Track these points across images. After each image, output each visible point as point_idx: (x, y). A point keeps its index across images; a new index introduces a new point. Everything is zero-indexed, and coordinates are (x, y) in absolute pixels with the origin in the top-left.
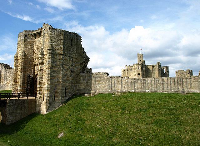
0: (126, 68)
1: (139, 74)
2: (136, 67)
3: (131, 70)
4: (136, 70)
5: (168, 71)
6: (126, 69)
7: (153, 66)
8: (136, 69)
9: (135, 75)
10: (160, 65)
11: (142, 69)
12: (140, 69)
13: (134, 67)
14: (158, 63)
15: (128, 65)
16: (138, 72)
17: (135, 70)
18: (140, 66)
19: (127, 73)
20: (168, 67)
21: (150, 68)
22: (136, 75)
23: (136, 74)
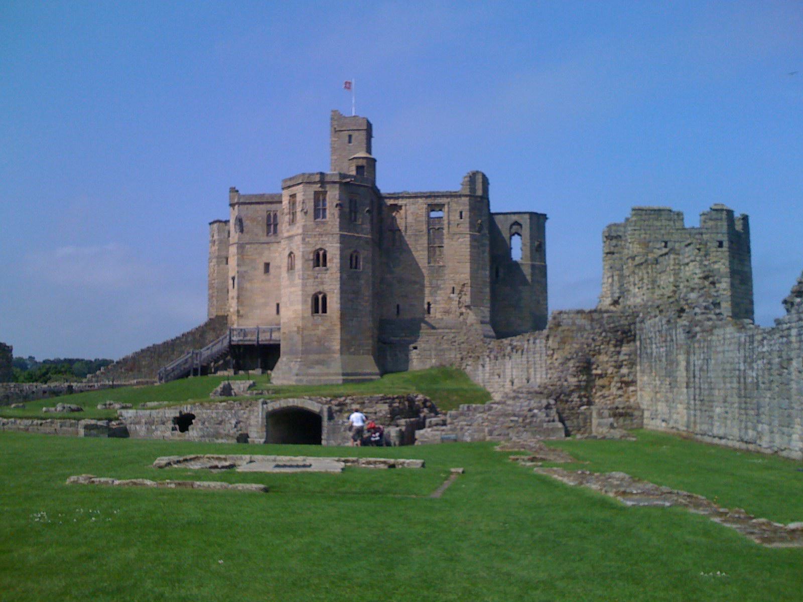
0: (232, 215)
1: (319, 259)
2: (299, 198)
3: (271, 224)
4: (297, 229)
5: (538, 249)
6: (232, 222)
7: (435, 201)
8: (299, 215)
9: (291, 267)
10: (484, 199)
11: (349, 215)
12: (332, 214)
13: (286, 200)
14: (472, 177)
15: (247, 189)
16: (315, 243)
17: (292, 222)
18: (333, 195)
19: (241, 247)
20: (538, 220)
21: (410, 217)
22: (299, 264)
23: (298, 254)
